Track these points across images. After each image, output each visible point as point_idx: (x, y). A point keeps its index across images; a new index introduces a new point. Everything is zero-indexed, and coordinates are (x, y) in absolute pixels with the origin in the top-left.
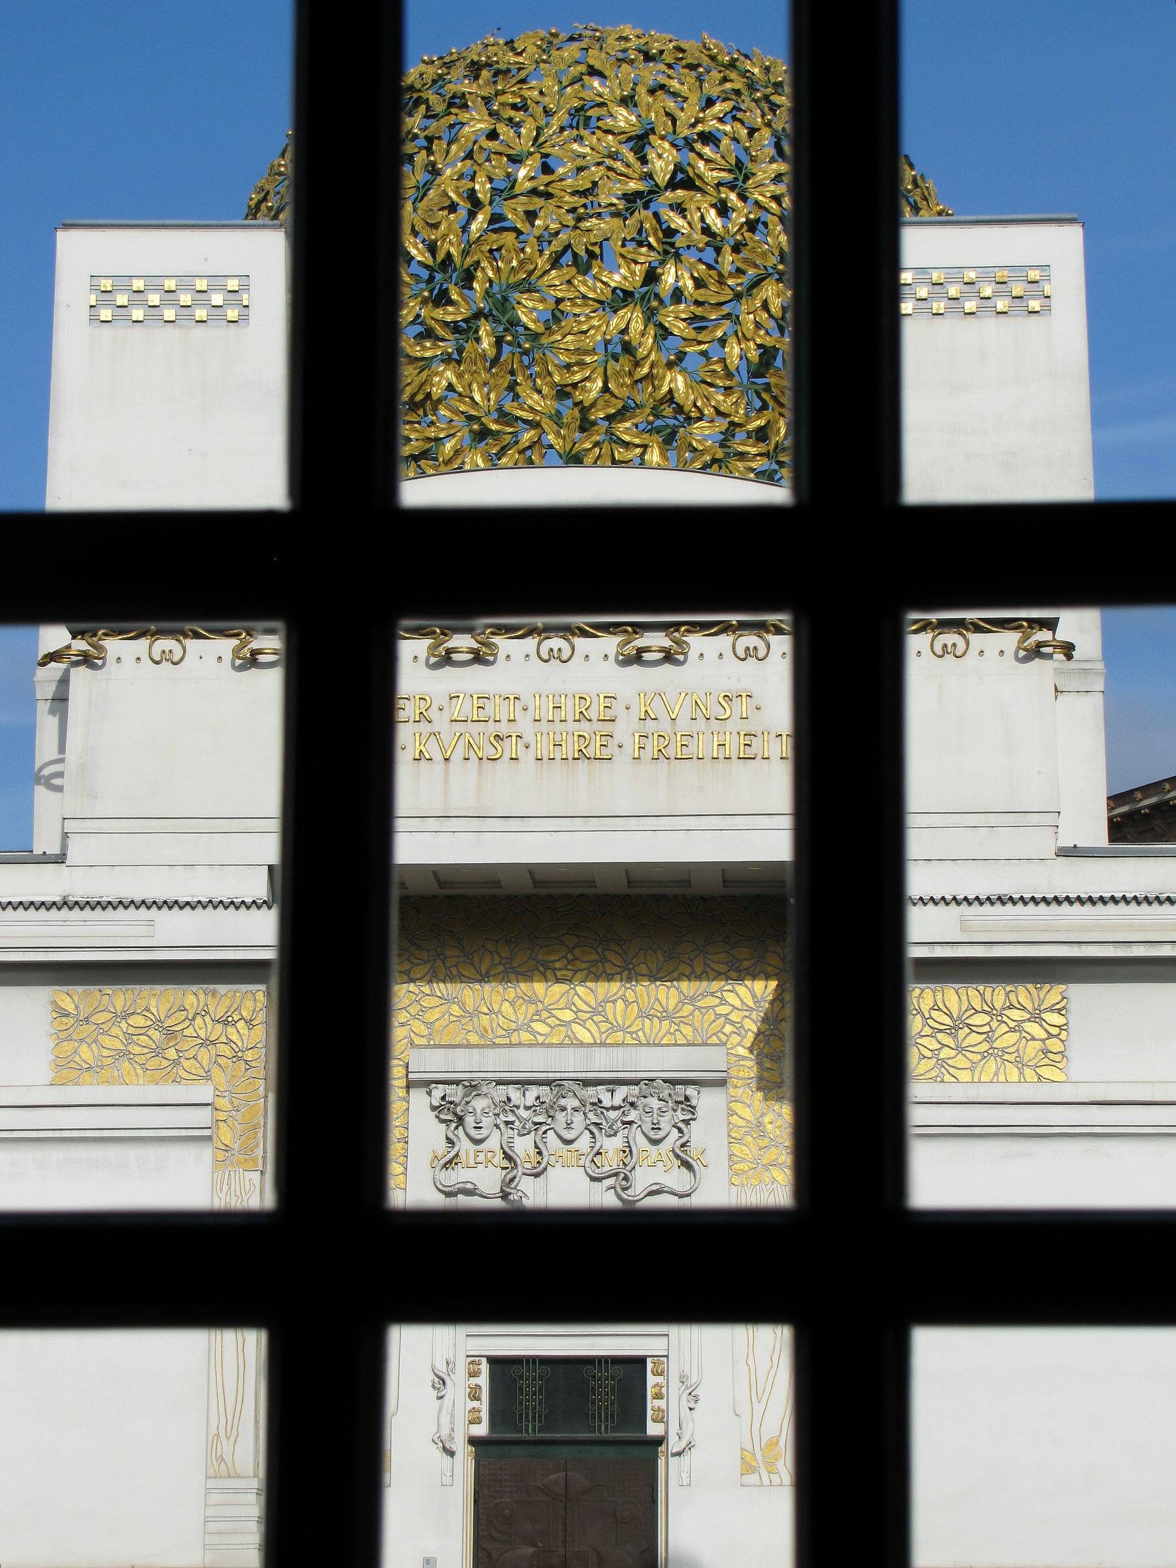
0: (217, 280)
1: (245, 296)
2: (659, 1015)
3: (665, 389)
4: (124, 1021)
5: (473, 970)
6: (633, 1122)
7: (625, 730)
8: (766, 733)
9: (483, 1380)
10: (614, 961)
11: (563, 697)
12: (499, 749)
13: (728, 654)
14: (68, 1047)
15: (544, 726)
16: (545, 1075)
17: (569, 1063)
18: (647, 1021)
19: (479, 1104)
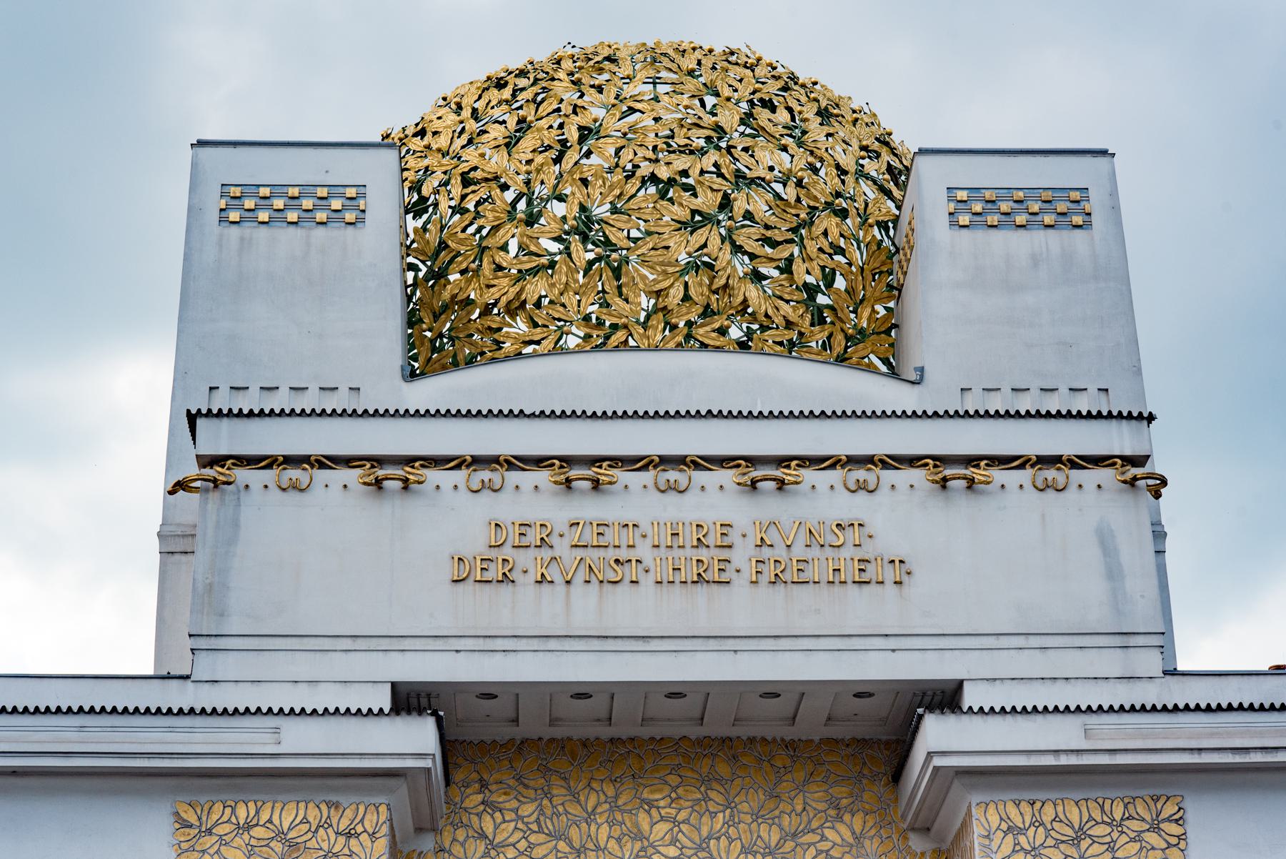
0: (335, 189)
1: (362, 202)
2: (762, 850)
3: (740, 299)
4: (246, 833)
5: (579, 808)
7: (742, 556)
8: (879, 559)
10: (716, 800)
11: (681, 524)
12: (620, 572)
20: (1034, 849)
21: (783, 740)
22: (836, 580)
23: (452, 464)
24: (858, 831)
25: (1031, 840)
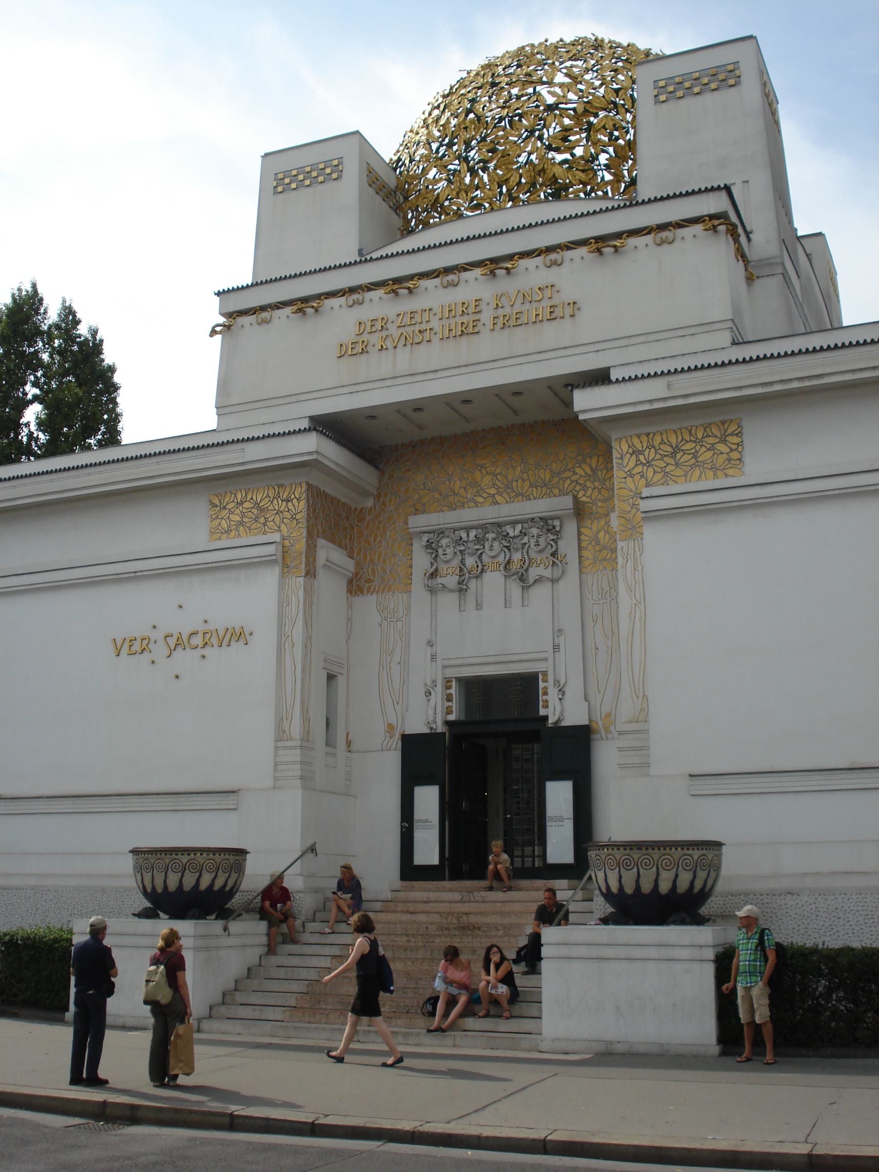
6: (526, 543)
7: (486, 317)
9: (453, 691)
13: (541, 266)
14: (217, 522)
15: (444, 321)
16: (477, 522)
17: (488, 513)
18: (534, 489)
19: (444, 542)
20: (648, 462)
21: (553, 420)
22: (538, 321)
23: (340, 294)
24: (594, 467)
25: (647, 457)
